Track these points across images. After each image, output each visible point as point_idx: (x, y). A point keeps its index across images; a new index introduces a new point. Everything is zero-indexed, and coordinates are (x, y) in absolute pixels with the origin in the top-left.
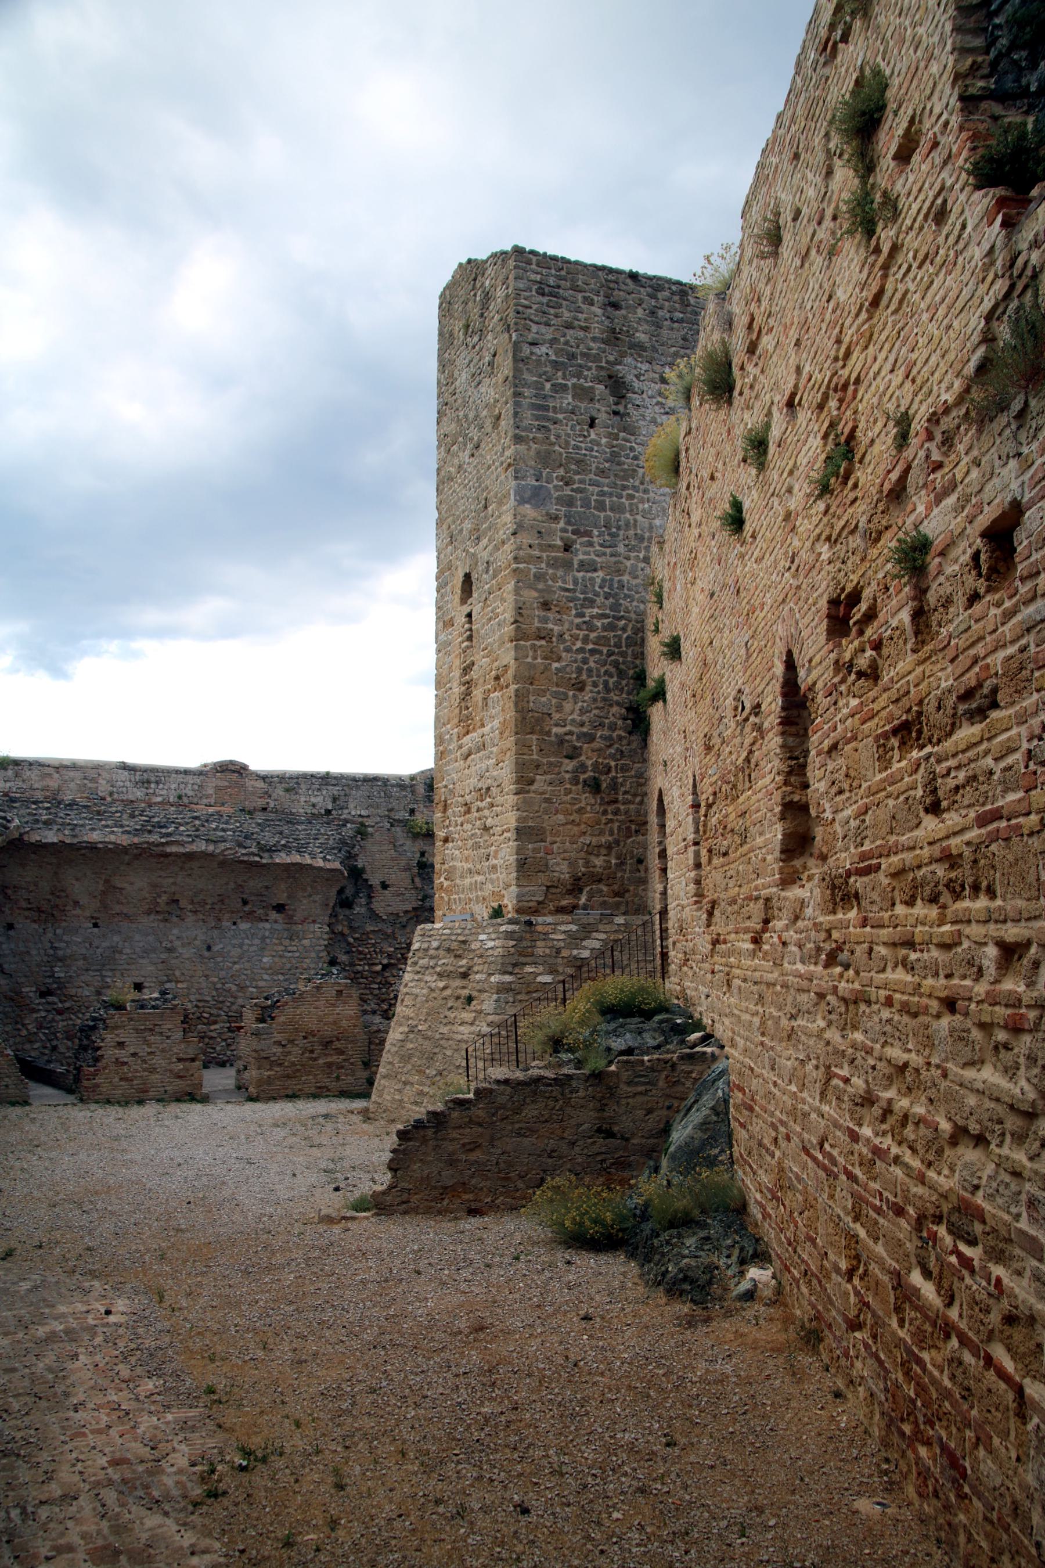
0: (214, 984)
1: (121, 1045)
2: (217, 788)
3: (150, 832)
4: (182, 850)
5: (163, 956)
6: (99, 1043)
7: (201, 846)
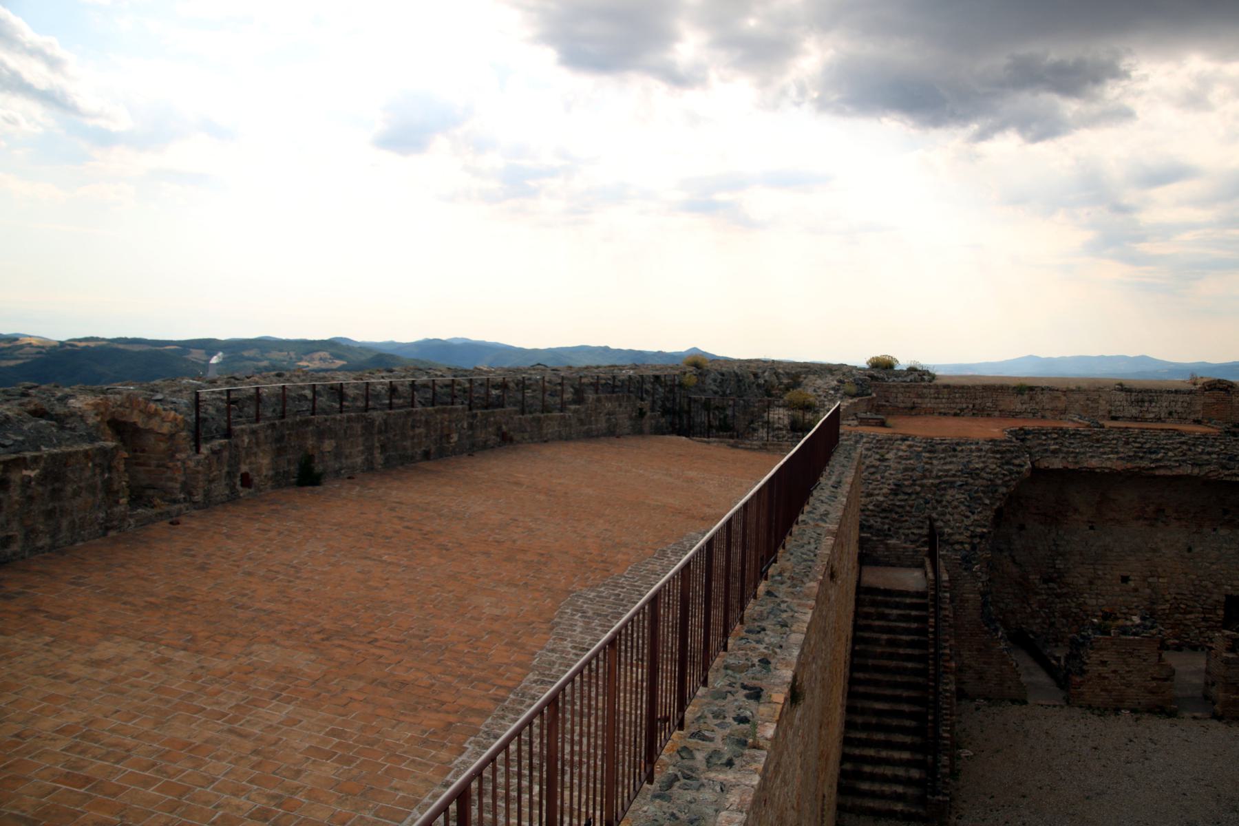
0: (1192, 580)
1: (1104, 663)
2: (1205, 405)
3: (1141, 458)
4: (1169, 473)
5: (1148, 555)
6: (1085, 659)
7: (1187, 470)
